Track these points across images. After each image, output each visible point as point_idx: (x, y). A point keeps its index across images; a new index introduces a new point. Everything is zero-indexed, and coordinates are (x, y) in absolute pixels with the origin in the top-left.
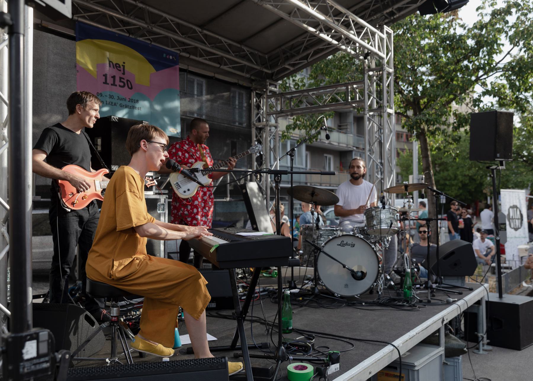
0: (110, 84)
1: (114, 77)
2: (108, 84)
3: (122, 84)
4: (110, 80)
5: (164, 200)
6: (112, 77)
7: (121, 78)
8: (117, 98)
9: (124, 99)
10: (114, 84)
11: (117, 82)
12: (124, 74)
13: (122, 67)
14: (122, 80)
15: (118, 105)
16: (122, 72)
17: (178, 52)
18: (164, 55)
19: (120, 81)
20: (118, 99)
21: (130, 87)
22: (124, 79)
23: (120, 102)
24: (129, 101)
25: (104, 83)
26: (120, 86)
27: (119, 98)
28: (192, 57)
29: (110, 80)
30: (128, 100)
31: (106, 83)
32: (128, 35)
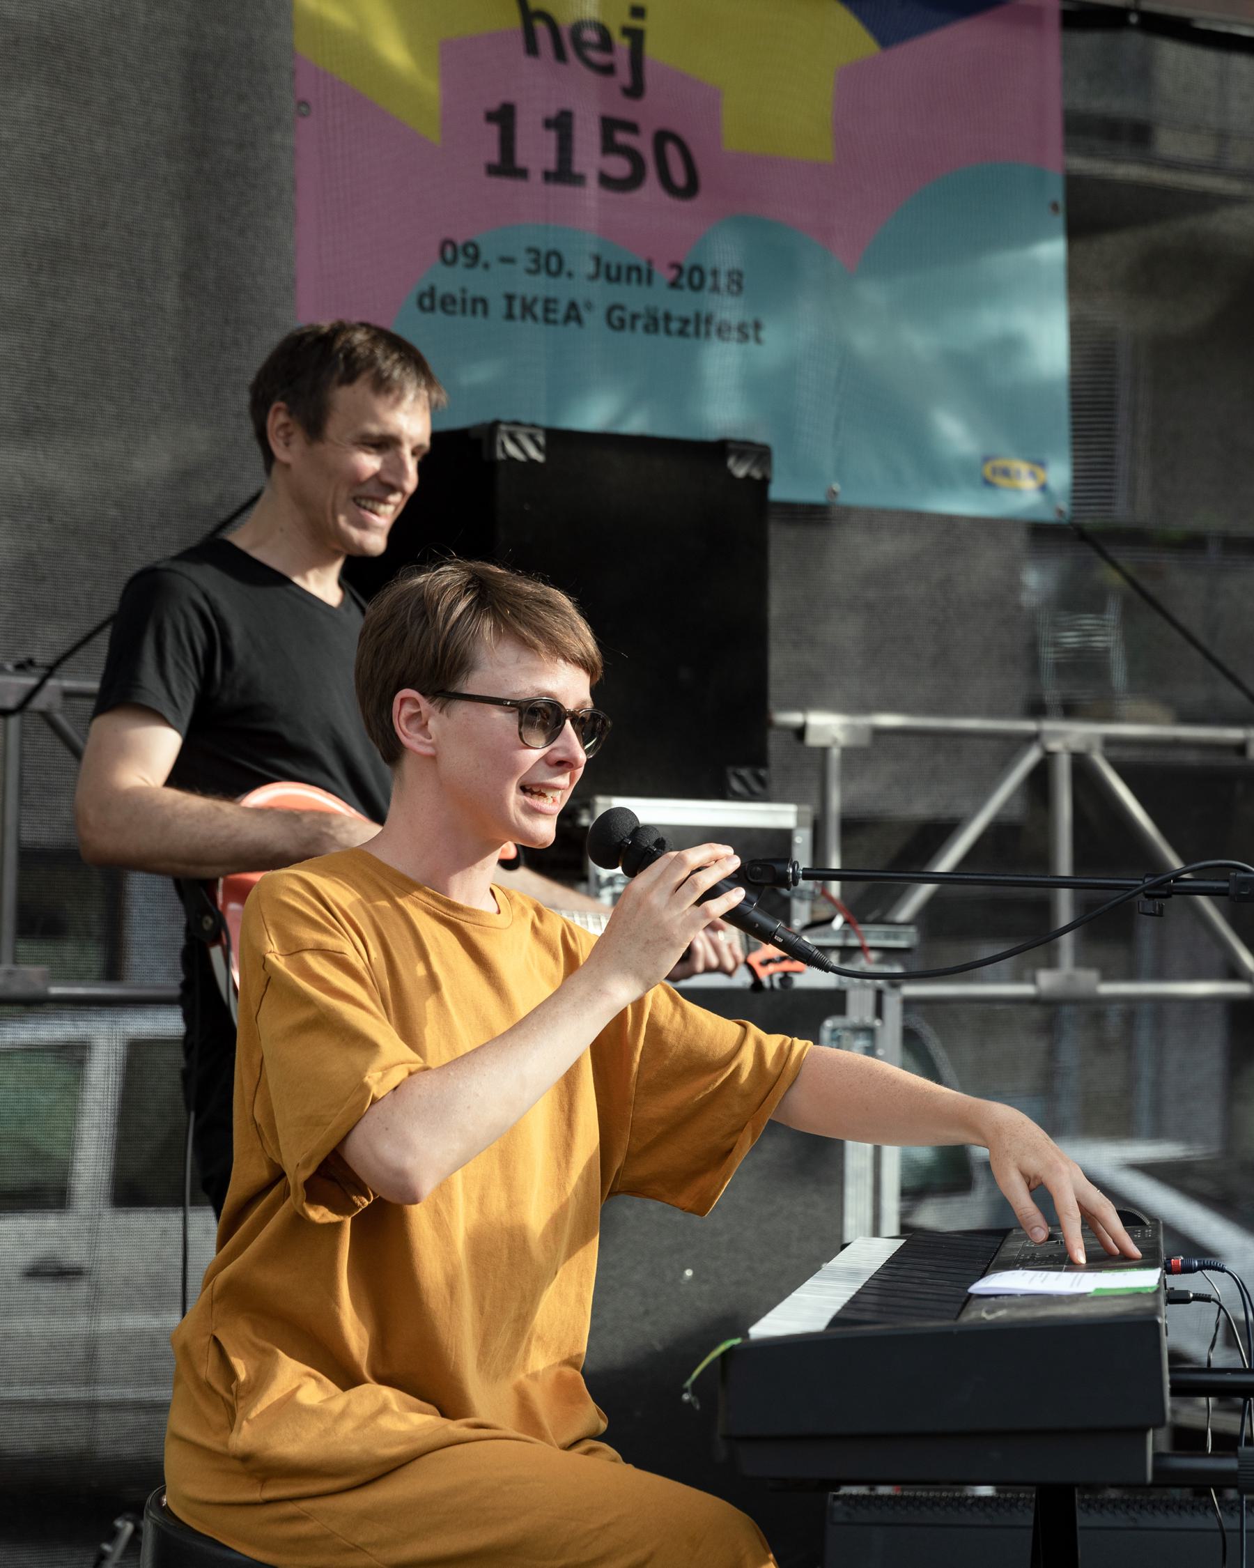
0: (536, 177)
1: (562, 124)
2: (522, 174)
3: (619, 167)
5: (870, 997)
6: (548, 124)
7: (609, 126)
8: (590, 267)
9: (640, 274)
10: (563, 173)
12: (635, 90)
13: (622, 44)
14: (622, 138)
15: (594, 320)
16: (624, 75)
19: (609, 147)
20: (595, 277)
21: (679, 178)
22: (632, 128)
24: (674, 285)
25: (493, 170)
30: (663, 276)
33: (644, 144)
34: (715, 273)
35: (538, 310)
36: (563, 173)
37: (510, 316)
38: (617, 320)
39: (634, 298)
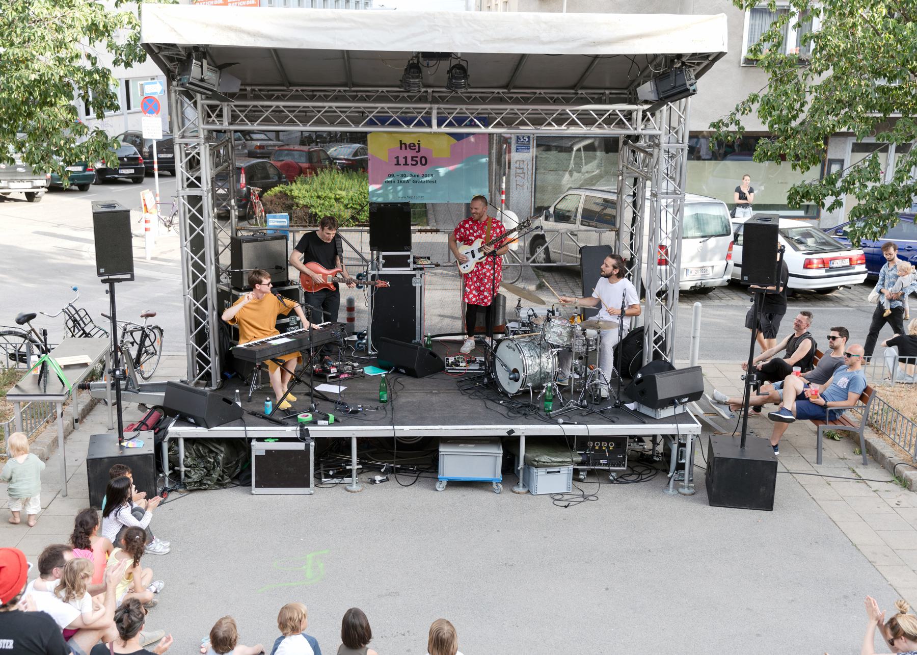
1: (406, 158)
3: (414, 163)
4: (402, 161)
7: (412, 157)
9: (418, 176)
10: (406, 164)
11: (409, 161)
12: (419, 151)
13: (417, 145)
16: (417, 150)
19: (412, 160)
21: (424, 163)
26: (412, 165)
29: (402, 161)
30: (421, 176)
31: (398, 164)
33: (418, 159)
39: (416, 179)
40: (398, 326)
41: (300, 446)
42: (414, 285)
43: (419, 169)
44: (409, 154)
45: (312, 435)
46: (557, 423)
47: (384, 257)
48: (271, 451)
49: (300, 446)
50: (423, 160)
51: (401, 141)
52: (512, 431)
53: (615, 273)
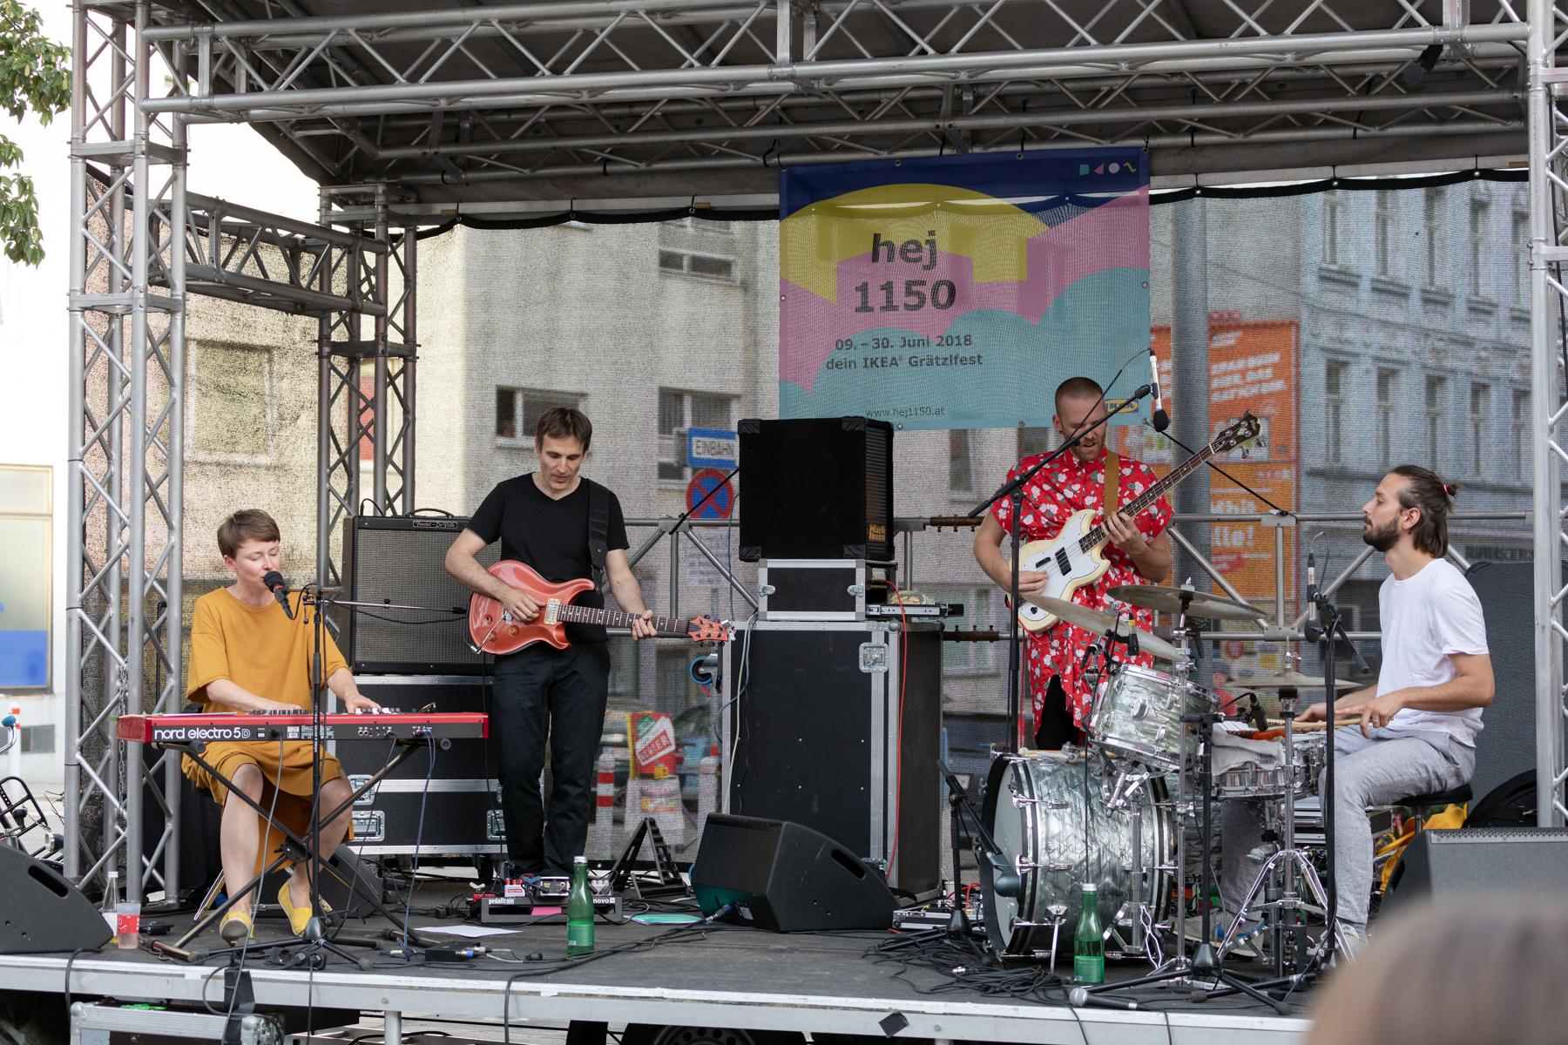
0: (877, 307)
3: (914, 300)
4: (877, 298)
7: (909, 284)
10: (889, 306)
11: (899, 297)
14: (915, 288)
15: (904, 364)
16: (926, 260)
17: (1140, 142)
18: (1084, 169)
19: (909, 292)
22: (922, 283)
23: (908, 352)
26: (907, 307)
27: (906, 343)
28: (1199, 139)
29: (877, 298)
30: (934, 341)
31: (865, 308)
32: (936, 152)
33: (927, 290)
34: (958, 337)
35: (879, 363)
36: (889, 306)
37: (866, 366)
38: (913, 362)
39: (921, 352)
40: (816, 809)
41: (214, 1027)
42: (863, 668)
43: (930, 320)
44: (900, 273)
45: (263, 995)
46: (1066, 1002)
47: (774, 576)
48: (129, 1035)
49: (214, 1027)
50: (944, 290)
51: (877, 237)
52: (896, 1020)
53: (1408, 525)
